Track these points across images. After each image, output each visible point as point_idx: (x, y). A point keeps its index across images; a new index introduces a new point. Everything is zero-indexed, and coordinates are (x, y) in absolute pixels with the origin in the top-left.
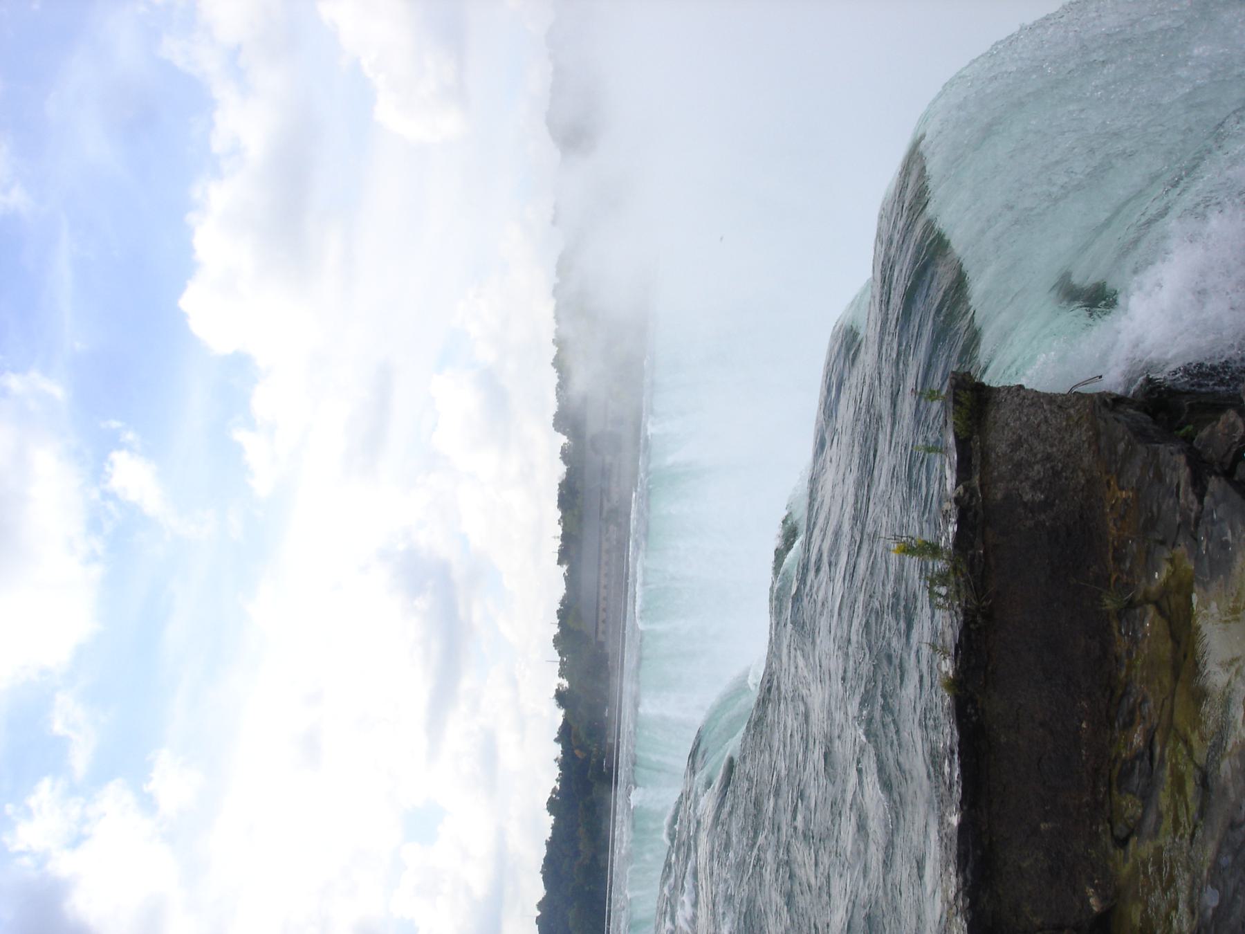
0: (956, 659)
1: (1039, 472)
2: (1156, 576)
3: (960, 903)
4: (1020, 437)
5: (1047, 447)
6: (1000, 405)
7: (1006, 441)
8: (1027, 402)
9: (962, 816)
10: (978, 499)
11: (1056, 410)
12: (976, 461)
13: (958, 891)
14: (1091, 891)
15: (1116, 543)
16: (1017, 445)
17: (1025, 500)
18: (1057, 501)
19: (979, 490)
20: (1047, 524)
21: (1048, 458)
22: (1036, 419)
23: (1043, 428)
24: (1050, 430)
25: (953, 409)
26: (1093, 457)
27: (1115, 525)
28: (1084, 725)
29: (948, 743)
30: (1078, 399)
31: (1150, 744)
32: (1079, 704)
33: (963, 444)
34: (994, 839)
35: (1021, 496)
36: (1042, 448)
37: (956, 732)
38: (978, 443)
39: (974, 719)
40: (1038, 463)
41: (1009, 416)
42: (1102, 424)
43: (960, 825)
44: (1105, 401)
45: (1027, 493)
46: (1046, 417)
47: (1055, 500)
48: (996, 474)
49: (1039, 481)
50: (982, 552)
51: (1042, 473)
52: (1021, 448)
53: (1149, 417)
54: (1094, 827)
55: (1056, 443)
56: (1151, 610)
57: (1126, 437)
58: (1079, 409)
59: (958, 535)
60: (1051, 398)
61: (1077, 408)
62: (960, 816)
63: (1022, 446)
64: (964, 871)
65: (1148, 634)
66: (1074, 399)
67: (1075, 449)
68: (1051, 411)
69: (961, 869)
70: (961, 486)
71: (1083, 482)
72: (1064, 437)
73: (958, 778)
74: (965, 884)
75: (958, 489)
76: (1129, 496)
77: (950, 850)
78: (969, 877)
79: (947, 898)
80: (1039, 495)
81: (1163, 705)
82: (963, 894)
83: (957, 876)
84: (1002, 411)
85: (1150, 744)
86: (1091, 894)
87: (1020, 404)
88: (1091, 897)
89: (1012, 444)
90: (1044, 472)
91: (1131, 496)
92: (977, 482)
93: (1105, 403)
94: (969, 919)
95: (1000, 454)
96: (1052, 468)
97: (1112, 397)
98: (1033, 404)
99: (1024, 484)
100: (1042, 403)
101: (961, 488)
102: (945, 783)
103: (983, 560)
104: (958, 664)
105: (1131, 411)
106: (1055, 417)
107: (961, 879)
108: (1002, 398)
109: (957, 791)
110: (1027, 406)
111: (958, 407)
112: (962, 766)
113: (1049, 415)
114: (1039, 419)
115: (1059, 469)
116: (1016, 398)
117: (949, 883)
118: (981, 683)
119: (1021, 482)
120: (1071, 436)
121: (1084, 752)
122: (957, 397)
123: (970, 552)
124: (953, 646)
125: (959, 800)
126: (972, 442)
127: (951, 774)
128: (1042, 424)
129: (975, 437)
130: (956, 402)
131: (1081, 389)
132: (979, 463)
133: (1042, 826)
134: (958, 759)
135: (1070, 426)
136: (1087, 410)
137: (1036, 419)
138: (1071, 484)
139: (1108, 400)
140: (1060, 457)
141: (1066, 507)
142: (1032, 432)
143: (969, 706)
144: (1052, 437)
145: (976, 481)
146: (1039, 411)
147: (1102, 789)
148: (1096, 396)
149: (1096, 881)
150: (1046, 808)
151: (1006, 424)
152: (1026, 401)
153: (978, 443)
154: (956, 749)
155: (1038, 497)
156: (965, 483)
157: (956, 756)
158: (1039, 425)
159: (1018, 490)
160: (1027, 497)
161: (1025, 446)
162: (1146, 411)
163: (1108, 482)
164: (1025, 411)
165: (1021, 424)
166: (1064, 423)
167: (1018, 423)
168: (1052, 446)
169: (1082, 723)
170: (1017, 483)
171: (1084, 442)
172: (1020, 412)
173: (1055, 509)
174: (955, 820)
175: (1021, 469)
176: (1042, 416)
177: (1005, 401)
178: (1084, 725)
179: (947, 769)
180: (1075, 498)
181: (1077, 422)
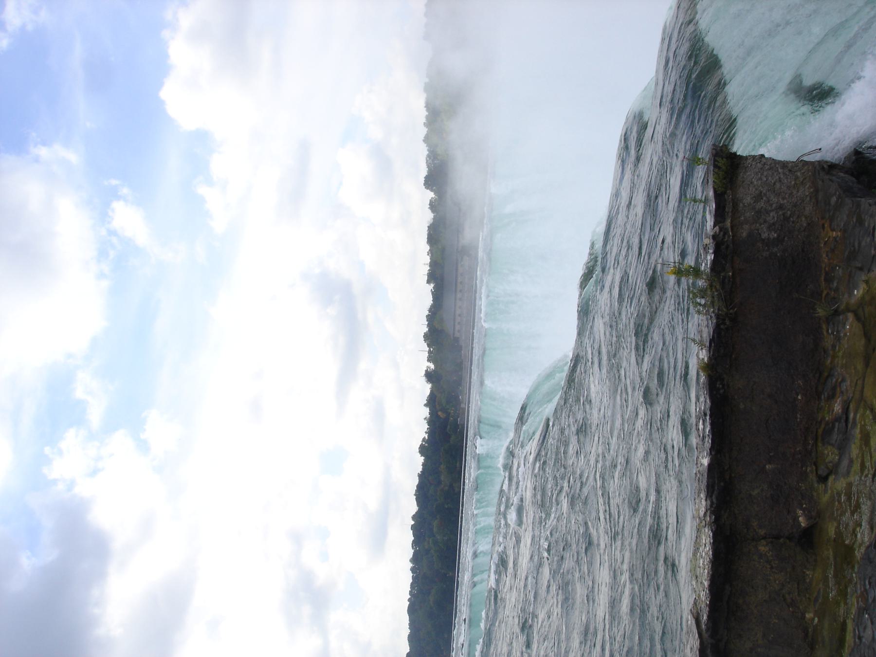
0: (710, 349)
1: (774, 218)
2: (856, 292)
4: (761, 192)
5: (780, 199)
6: (747, 169)
7: (751, 195)
8: (767, 167)
9: (711, 459)
10: (729, 236)
11: (787, 173)
12: (729, 208)
14: (800, 512)
15: (827, 269)
16: (759, 197)
17: (763, 237)
18: (786, 239)
19: (730, 230)
20: (778, 255)
21: (781, 207)
22: (773, 179)
23: (778, 185)
24: (783, 187)
25: (714, 171)
26: (813, 207)
27: (827, 256)
28: (799, 397)
29: (703, 408)
30: (803, 166)
31: (846, 411)
32: (796, 383)
33: (719, 197)
34: (733, 475)
35: (760, 235)
36: (776, 200)
37: (708, 401)
38: (731, 196)
39: (722, 391)
40: (773, 211)
41: (753, 177)
42: (820, 183)
43: (709, 465)
44: (823, 166)
45: (764, 233)
46: (780, 178)
47: (784, 237)
48: (742, 218)
49: (774, 224)
50: (731, 274)
51: (776, 218)
52: (762, 200)
53: (854, 179)
54: (804, 468)
55: (787, 196)
56: (851, 316)
57: (838, 193)
58: (804, 173)
59: (714, 262)
60: (784, 164)
61: (802, 171)
62: (709, 459)
63: (762, 199)
64: (711, 496)
65: (848, 334)
66: (800, 165)
67: (800, 201)
68: (784, 173)
69: (709, 495)
70: (717, 227)
71: (805, 225)
72: (793, 193)
73: (708, 432)
74: (711, 506)
75: (715, 229)
76: (838, 236)
78: (714, 500)
80: (773, 234)
81: (856, 383)
82: (710, 513)
83: (706, 500)
84: (749, 173)
85: (846, 411)
86: (800, 514)
87: (761, 169)
88: (800, 516)
89: (754, 197)
90: (777, 218)
91: (839, 236)
92: (729, 224)
93: (823, 168)
94: (714, 530)
95: (746, 204)
96: (784, 214)
97: (829, 164)
98: (771, 169)
99: (762, 226)
100: (777, 168)
101: (717, 228)
103: (731, 280)
104: (712, 353)
105: (842, 174)
106: (787, 178)
107: (709, 502)
108: (749, 163)
109: (708, 441)
110: (766, 170)
111: (716, 170)
112: (712, 424)
113: (782, 177)
114: (774, 179)
115: (788, 215)
116: (758, 164)
117: (701, 505)
118: (727, 366)
119: (761, 224)
120: (798, 191)
121: (799, 416)
122: (716, 163)
123: (722, 274)
124: (708, 340)
126: (726, 195)
127: (704, 429)
128: (777, 183)
129: (728, 191)
130: (715, 166)
131: (806, 158)
132: (730, 210)
133: (767, 467)
134: (709, 419)
135: (797, 184)
136: (810, 173)
137: (773, 179)
138: (796, 226)
139: (825, 166)
140: (788, 207)
141: (792, 242)
142: (769, 188)
143: (718, 383)
144: (784, 192)
145: (728, 223)
146: (775, 174)
147: (810, 442)
148: (817, 163)
149: (804, 506)
150: (771, 454)
151: (751, 183)
152: (766, 166)
153: (731, 196)
154: (708, 413)
155: (772, 235)
156: (720, 225)
157: (708, 418)
158: (775, 184)
159: (758, 230)
160: (764, 236)
161: (764, 198)
162: (852, 175)
163: (823, 225)
164: (765, 173)
165: (761, 183)
166: (793, 182)
167: (760, 182)
168: (783, 199)
169: (798, 395)
170: (758, 225)
171: (807, 196)
172: (761, 175)
173: (784, 244)
174: (706, 462)
175: (761, 215)
176: (777, 177)
177: (751, 166)
178: (799, 397)
179: (701, 426)
180: (799, 236)
181: (802, 182)
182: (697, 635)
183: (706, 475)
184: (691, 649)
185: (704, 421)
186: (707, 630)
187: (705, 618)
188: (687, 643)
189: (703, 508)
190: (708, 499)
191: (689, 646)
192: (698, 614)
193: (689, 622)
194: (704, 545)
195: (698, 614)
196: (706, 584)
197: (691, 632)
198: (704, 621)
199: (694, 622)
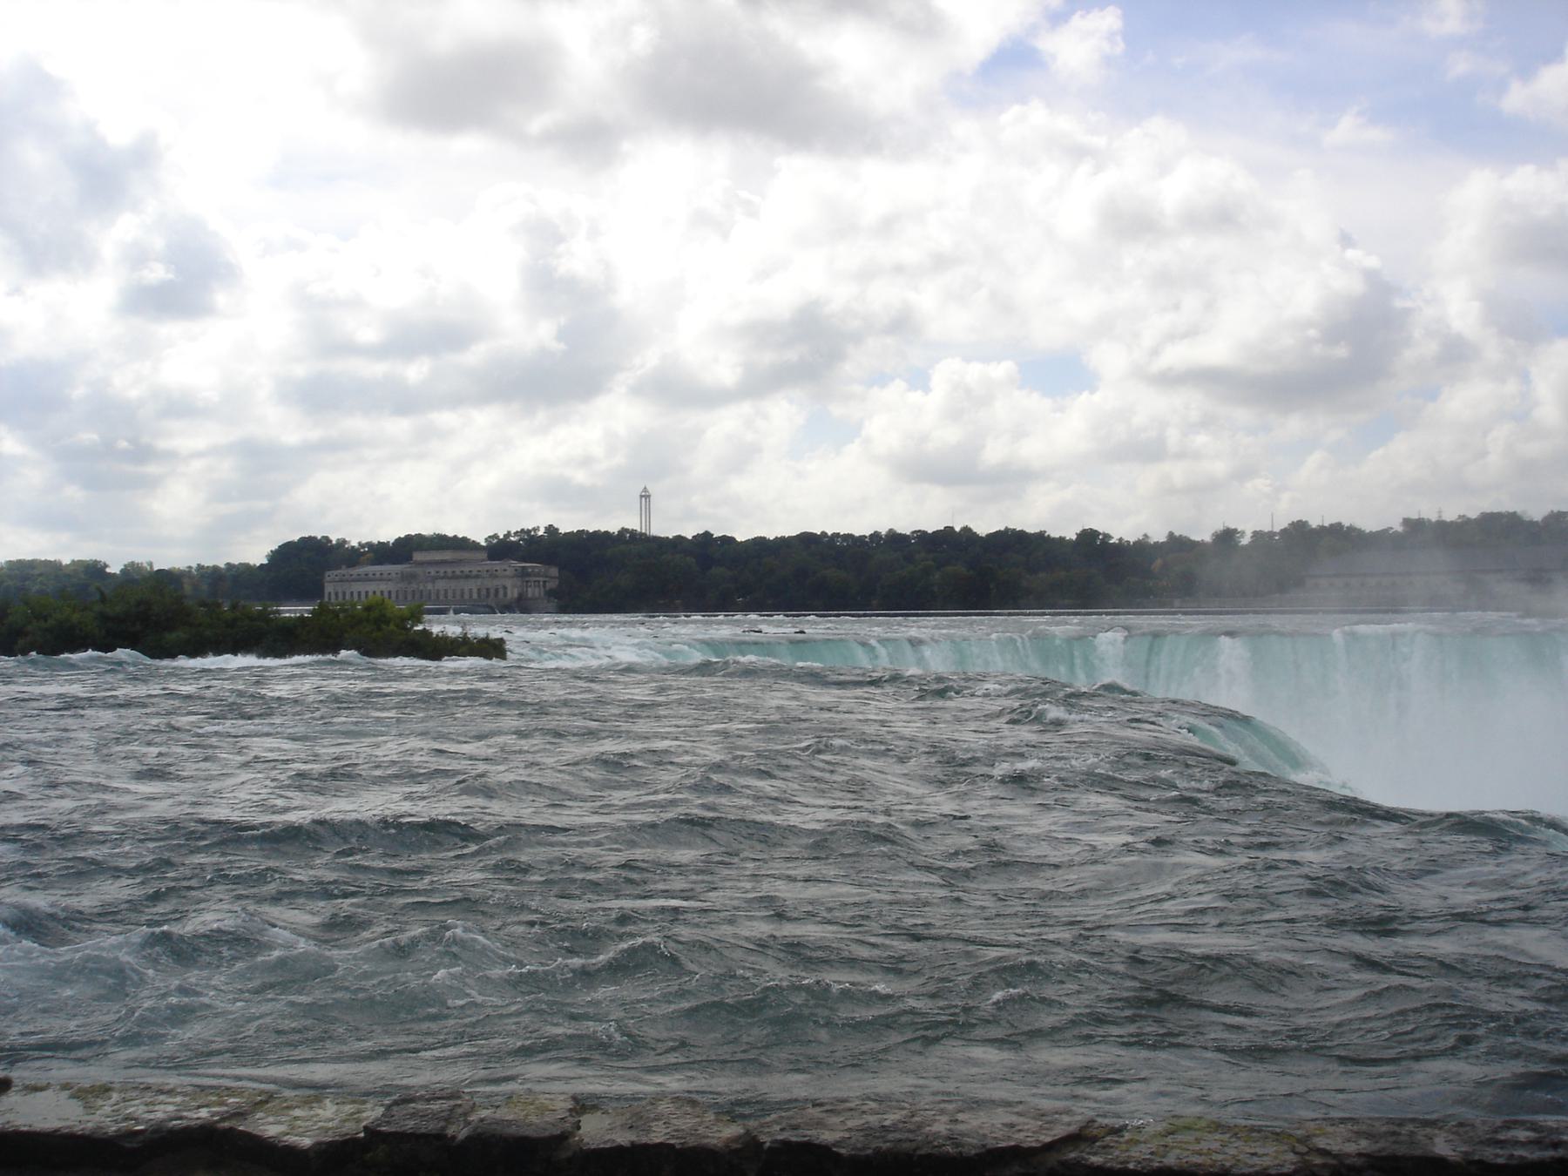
3: (1318, 1161)
13: (1335, 1156)
43: (1439, 1163)
62: (1458, 1159)
73: (1521, 1157)
74: (1351, 1168)
77: (1395, 1142)
79: (1315, 1135)
83: (1360, 1155)
102: (1496, 1131)
107: (1359, 1162)
109: (1497, 1156)
112: (1541, 1165)
117: (1339, 1140)
125: (1484, 1158)
127: (1516, 1143)
134: (1552, 1158)
157: (1549, 1154)
174: (1443, 1146)
182: (1048, 1139)
183: (1418, 1152)
184: (1012, 1126)
185: (1536, 1143)
186: (1063, 1164)
187: (1096, 1160)
188: (1019, 1114)
189: (1338, 1148)
190: (1363, 1160)
191: (1014, 1119)
192: (1094, 1139)
193: (1066, 1119)
194: (1253, 1151)
195: (1094, 1139)
196: (1170, 1160)
199: (1073, 1129)
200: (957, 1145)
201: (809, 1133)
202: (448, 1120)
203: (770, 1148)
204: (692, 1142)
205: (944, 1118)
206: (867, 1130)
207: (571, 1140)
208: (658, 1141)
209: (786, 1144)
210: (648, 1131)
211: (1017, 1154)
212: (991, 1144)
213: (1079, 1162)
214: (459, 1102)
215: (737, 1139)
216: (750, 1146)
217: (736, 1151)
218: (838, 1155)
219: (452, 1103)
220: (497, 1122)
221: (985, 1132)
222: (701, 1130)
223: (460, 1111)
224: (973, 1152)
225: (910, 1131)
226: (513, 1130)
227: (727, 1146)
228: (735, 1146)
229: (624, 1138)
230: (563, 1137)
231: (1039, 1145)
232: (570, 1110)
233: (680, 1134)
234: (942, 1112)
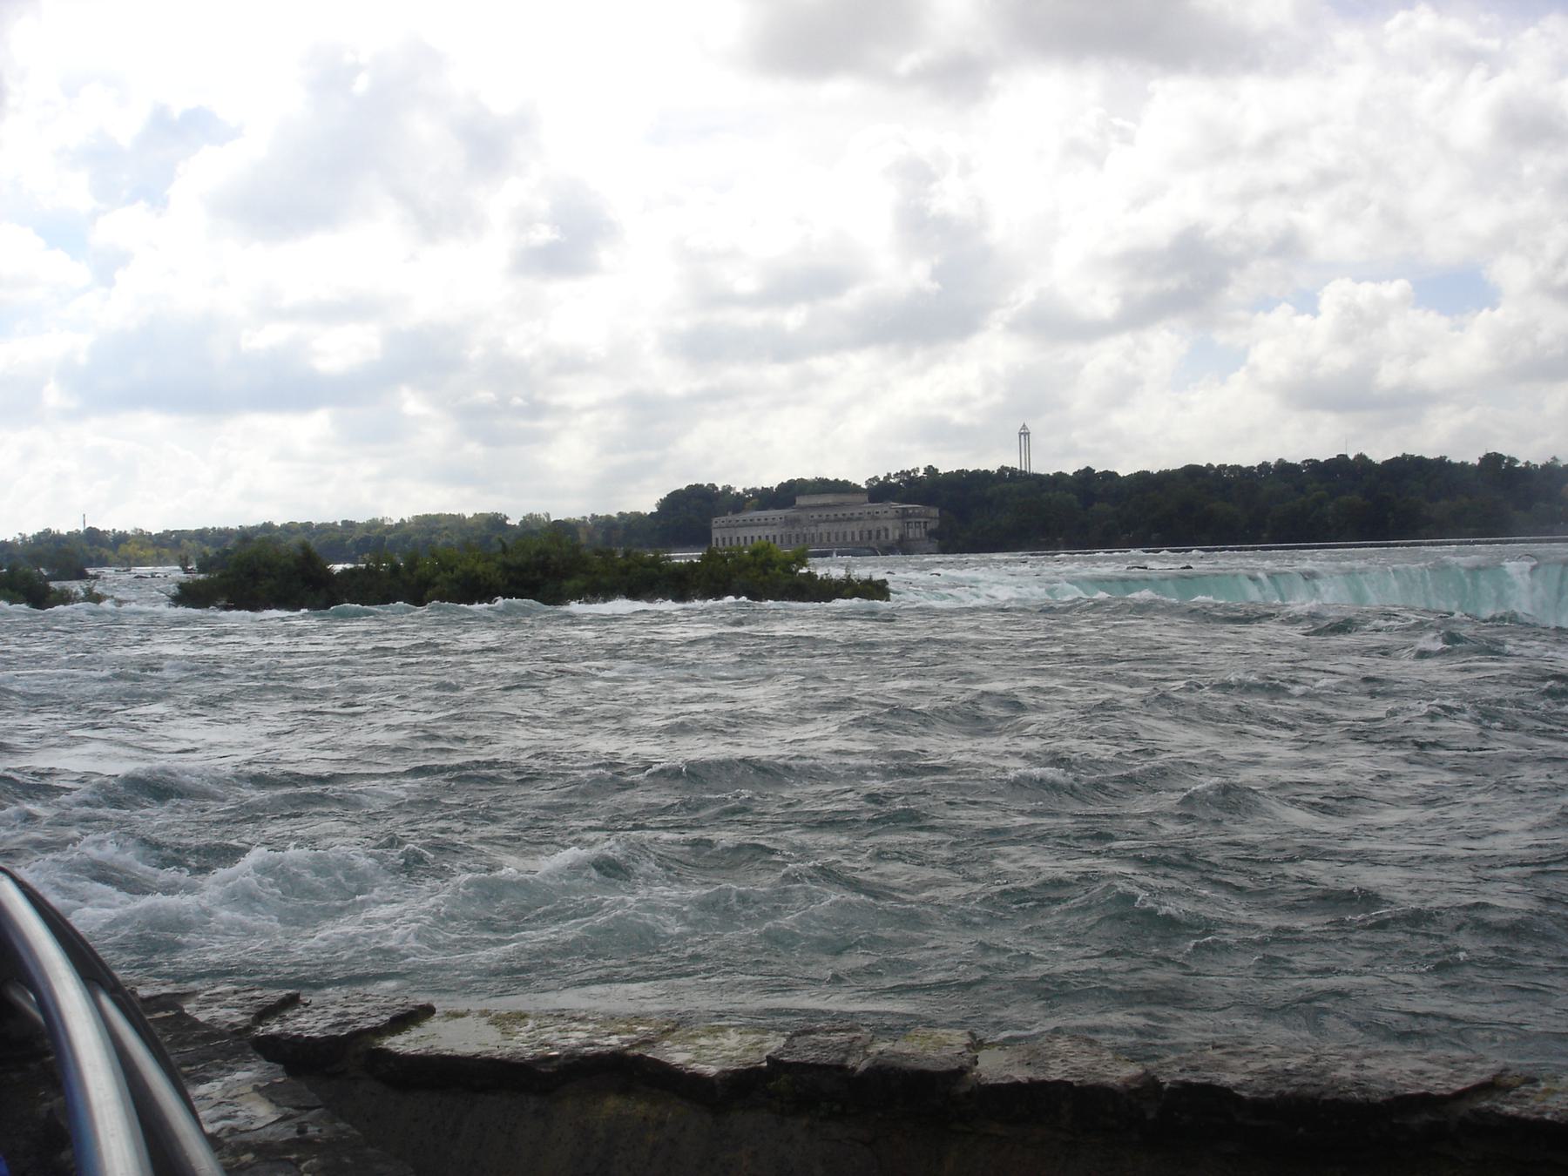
182: (1460, 1087)
184: (1421, 1073)
186: (1477, 1113)
187: (1510, 1109)
188: (1429, 1061)
191: (1422, 1065)
192: (1508, 1089)
193: (1478, 1066)
195: (1508, 1089)
197: (1460, 1070)
198: (1500, 1106)
199: (1485, 1077)
200: (1364, 1091)
201: (1209, 1074)
202: (847, 1052)
203: (1170, 1088)
204: (1090, 1080)
205: (1350, 1064)
206: (1269, 1073)
207: (969, 1075)
208: (1056, 1078)
209: (1186, 1085)
210: (1046, 1068)
211: (1426, 1101)
212: (1399, 1091)
213: (1491, 1111)
214: (859, 1034)
215: (1134, 1079)
216: (1149, 1085)
217: (1136, 1091)
218: (1241, 1098)
219: (852, 1035)
220: (896, 1055)
221: (1395, 1078)
222: (1099, 1068)
223: (859, 1043)
224: (1380, 1098)
225: (1313, 1076)
226: (911, 1064)
227: (1125, 1085)
228: (1134, 1086)
229: (1021, 1075)
230: (961, 1072)
231: (1450, 1093)
232: (967, 1045)
233: (1077, 1072)
234: (1348, 1057)
